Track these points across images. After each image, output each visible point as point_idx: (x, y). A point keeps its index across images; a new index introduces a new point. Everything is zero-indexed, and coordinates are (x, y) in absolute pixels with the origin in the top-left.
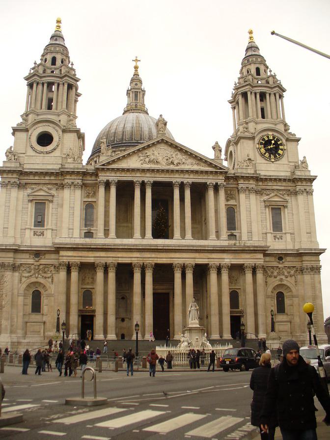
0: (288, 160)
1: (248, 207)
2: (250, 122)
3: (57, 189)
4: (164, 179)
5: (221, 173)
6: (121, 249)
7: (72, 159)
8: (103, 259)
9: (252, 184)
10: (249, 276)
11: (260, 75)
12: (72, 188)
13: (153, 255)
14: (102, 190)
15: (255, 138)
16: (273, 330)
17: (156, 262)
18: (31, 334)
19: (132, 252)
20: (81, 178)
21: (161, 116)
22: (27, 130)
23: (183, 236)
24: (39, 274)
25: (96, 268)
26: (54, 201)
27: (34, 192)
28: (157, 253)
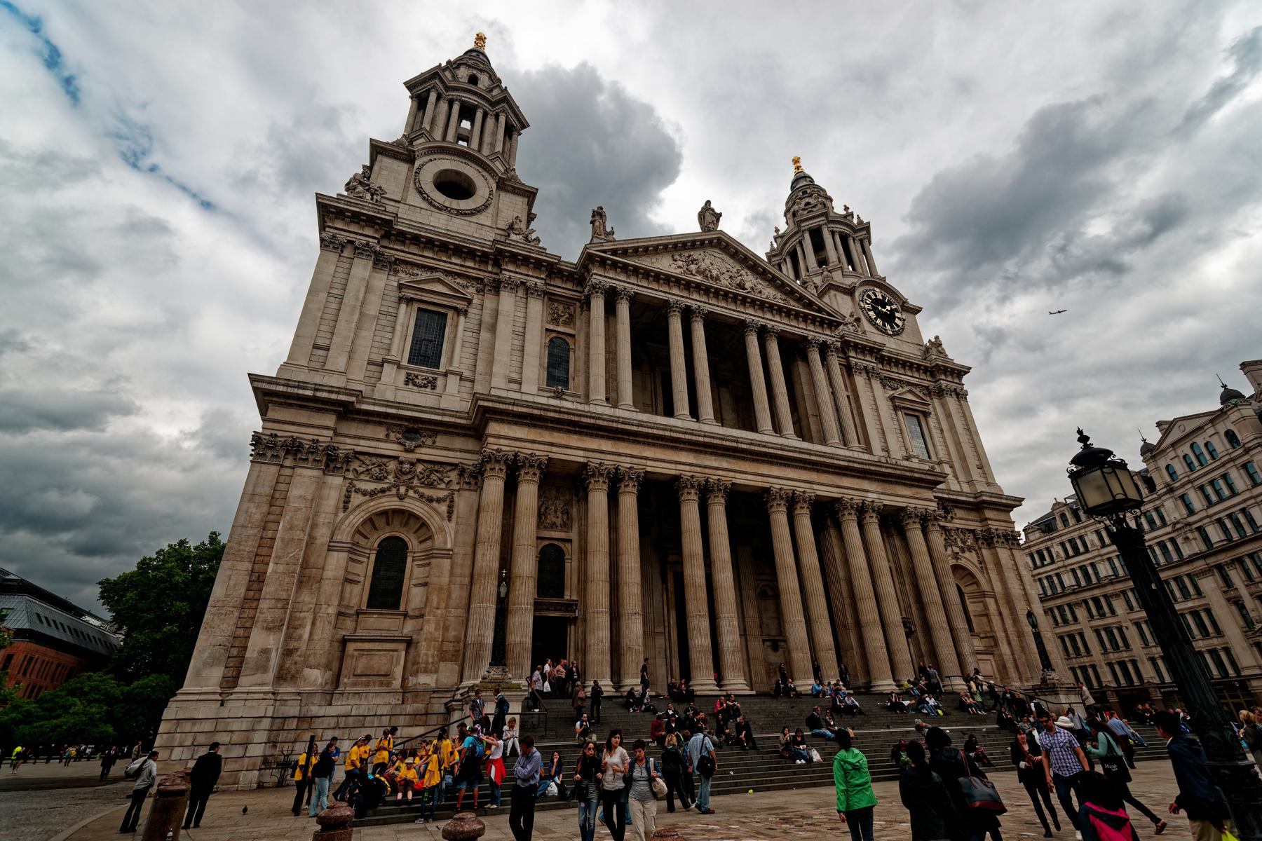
1: (873, 403)
2: (835, 270)
3: (478, 291)
4: (728, 311)
7: (521, 236)
8: (609, 457)
9: (871, 362)
13: (725, 464)
17: (734, 481)
18: (354, 684)
19: (676, 448)
20: (543, 276)
21: (708, 202)
22: (410, 159)
24: (409, 488)
25: (585, 479)
26: (469, 315)
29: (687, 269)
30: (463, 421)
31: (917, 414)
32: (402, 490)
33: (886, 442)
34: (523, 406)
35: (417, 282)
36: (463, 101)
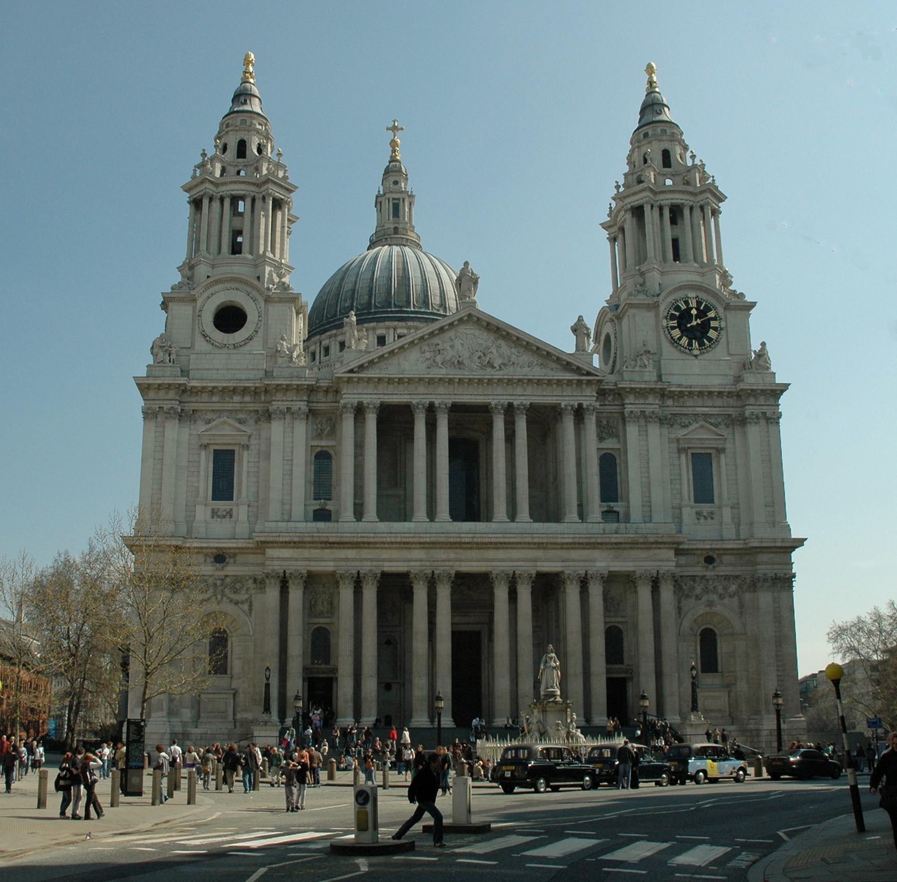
0: (728, 350)
2: (648, 271)
3: (256, 422)
4: (473, 397)
5: (589, 382)
6: (389, 543)
8: (354, 563)
9: (652, 405)
10: (644, 593)
11: (670, 167)
12: (288, 417)
13: (452, 554)
14: (348, 425)
15: (658, 306)
16: (694, 708)
19: (410, 548)
20: (305, 398)
23: (512, 515)
27: (210, 429)
28: (461, 551)
29: (434, 360)
30: (251, 546)
31: (708, 451)
32: (219, 597)
33: (650, 497)
34: (285, 536)
35: (210, 429)
36: (232, 195)
